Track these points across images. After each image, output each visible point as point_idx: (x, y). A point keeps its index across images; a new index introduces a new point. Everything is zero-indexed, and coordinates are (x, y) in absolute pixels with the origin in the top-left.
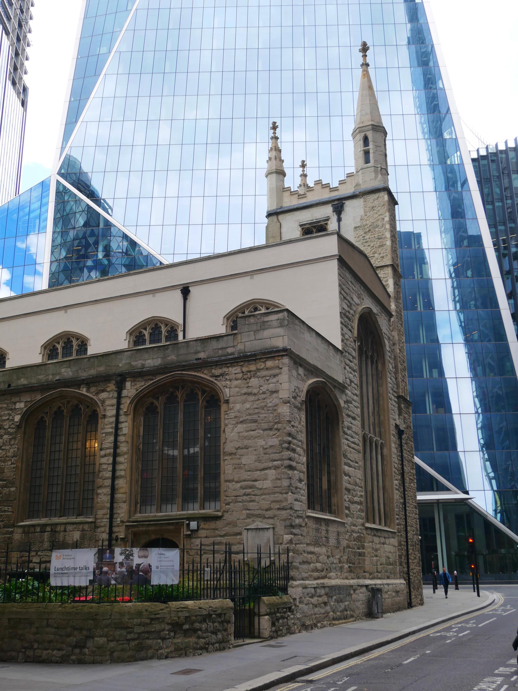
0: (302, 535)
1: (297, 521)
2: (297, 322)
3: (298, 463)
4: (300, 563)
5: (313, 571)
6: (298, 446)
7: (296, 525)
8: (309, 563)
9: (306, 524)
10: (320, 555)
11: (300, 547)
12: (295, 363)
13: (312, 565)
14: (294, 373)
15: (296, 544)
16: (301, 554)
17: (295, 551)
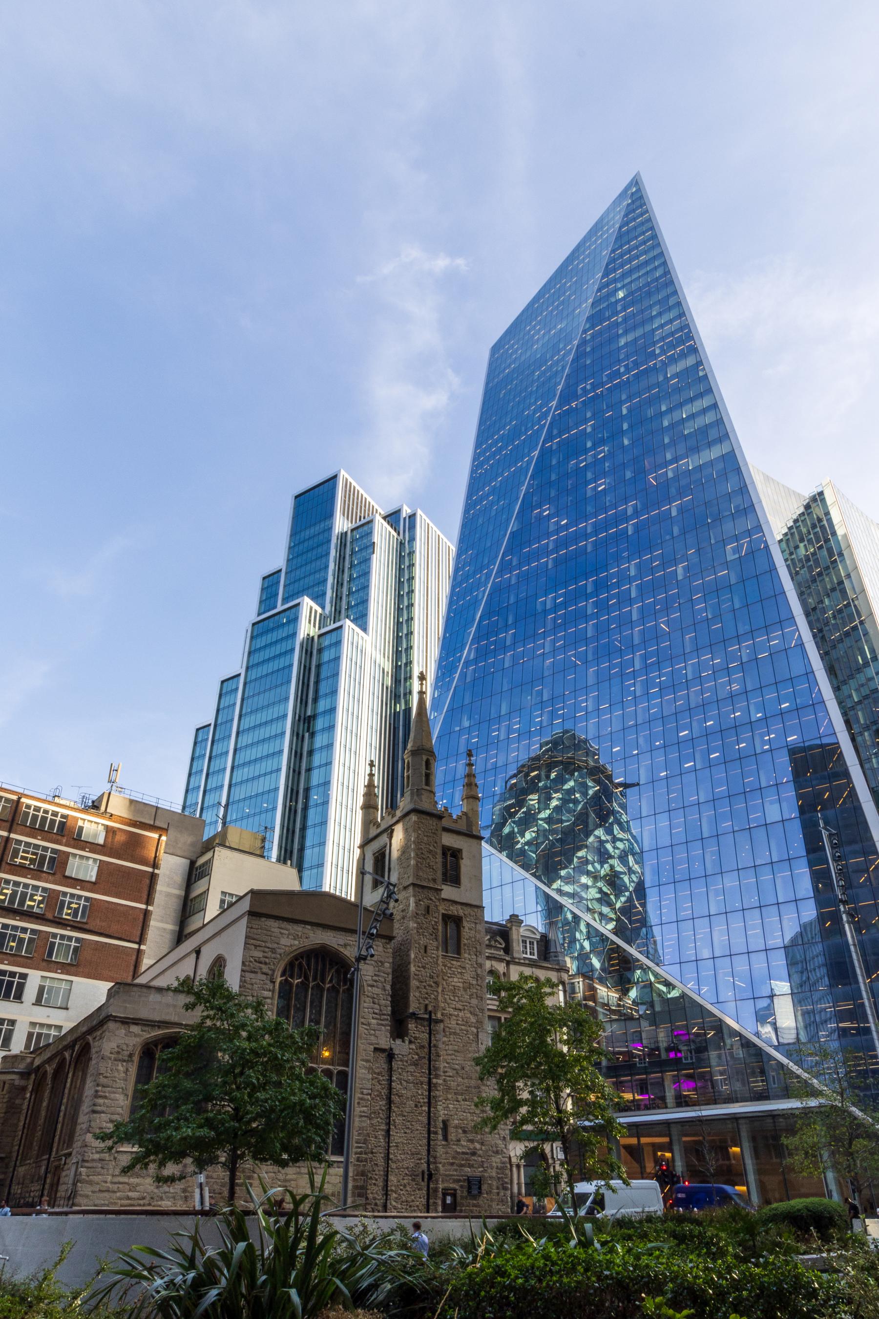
0: (102, 1168)
1: (96, 1156)
2: (135, 989)
3: (107, 1107)
4: (93, 1192)
5: (120, 1199)
6: (115, 1093)
7: (93, 1160)
8: (114, 1192)
9: (115, 1158)
10: (138, 1185)
11: (96, 1178)
12: (123, 1023)
13: (118, 1194)
14: (123, 1032)
15: (88, 1176)
16: (98, 1184)
17: (90, 1183)
